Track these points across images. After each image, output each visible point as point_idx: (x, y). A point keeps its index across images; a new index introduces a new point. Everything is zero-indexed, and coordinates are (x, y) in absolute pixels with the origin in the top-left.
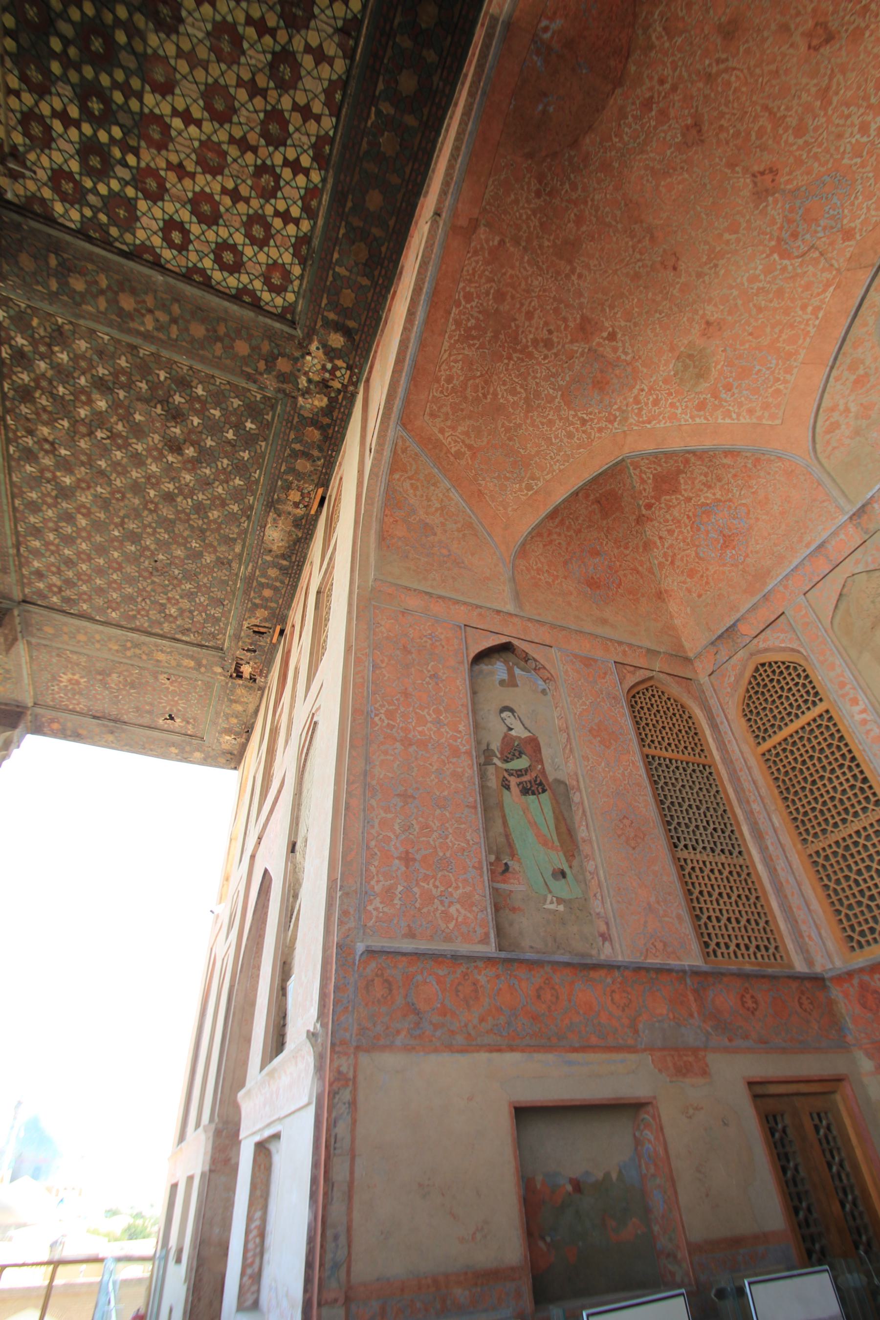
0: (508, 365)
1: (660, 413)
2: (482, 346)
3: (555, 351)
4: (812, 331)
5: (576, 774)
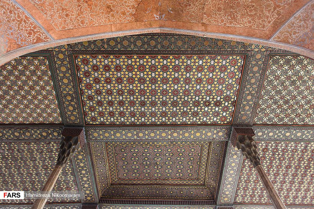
2: (236, 12)
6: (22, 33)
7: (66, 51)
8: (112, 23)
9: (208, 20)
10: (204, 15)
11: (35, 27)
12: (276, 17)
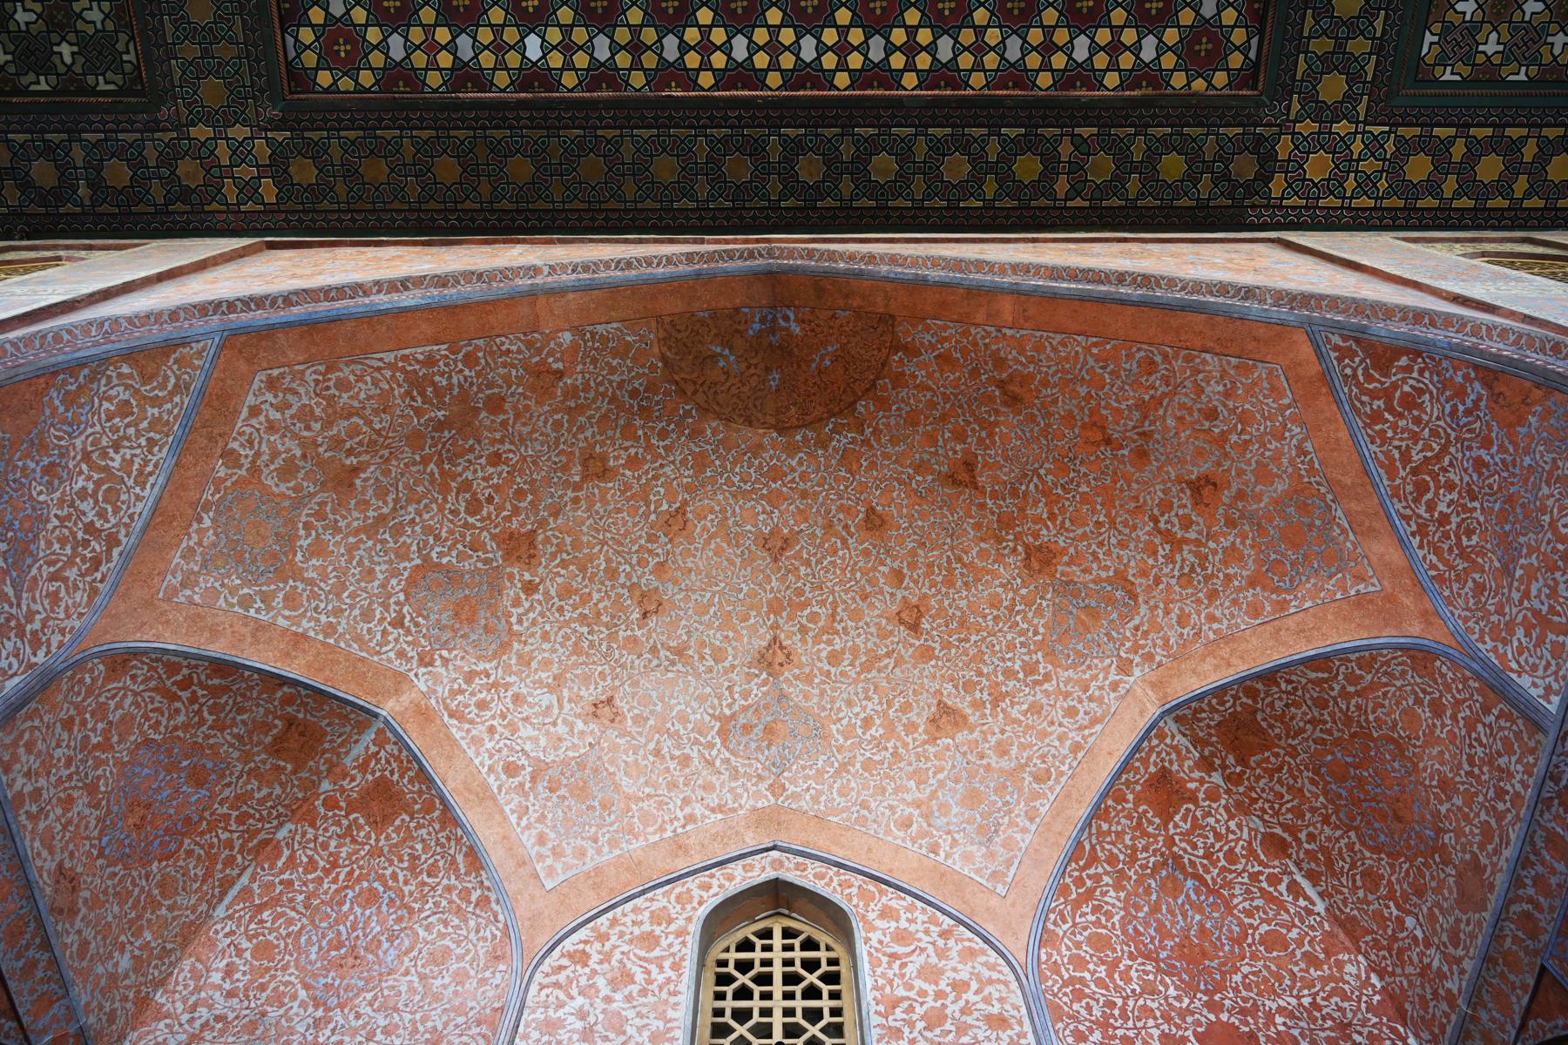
0: (415, 463)
1: (471, 722)
2: (418, 412)
3: (471, 520)
4: (669, 834)
6: (1441, 423)
7: (1295, 122)
8: (1009, 332)
9: (539, 351)
10: (560, 365)
11: (1376, 417)
12: (235, 439)
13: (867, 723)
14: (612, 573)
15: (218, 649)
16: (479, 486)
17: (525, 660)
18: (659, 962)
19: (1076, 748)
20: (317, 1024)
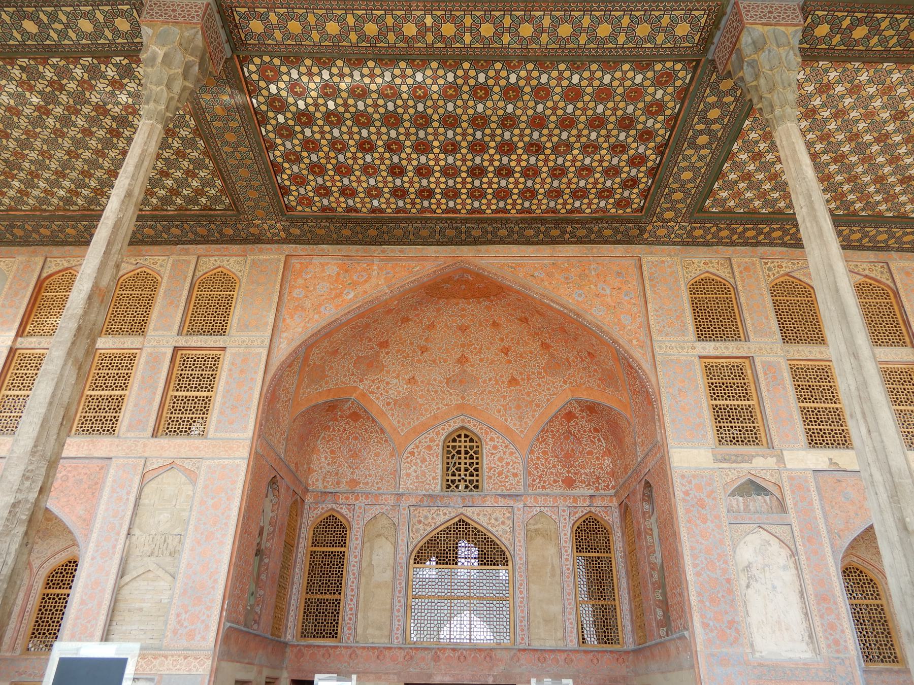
5: (270, 550)
13: (490, 380)
14: (412, 344)
15: (313, 404)
16: (371, 336)
17: (388, 372)
18: (432, 455)
19: (548, 400)
20: (352, 473)
